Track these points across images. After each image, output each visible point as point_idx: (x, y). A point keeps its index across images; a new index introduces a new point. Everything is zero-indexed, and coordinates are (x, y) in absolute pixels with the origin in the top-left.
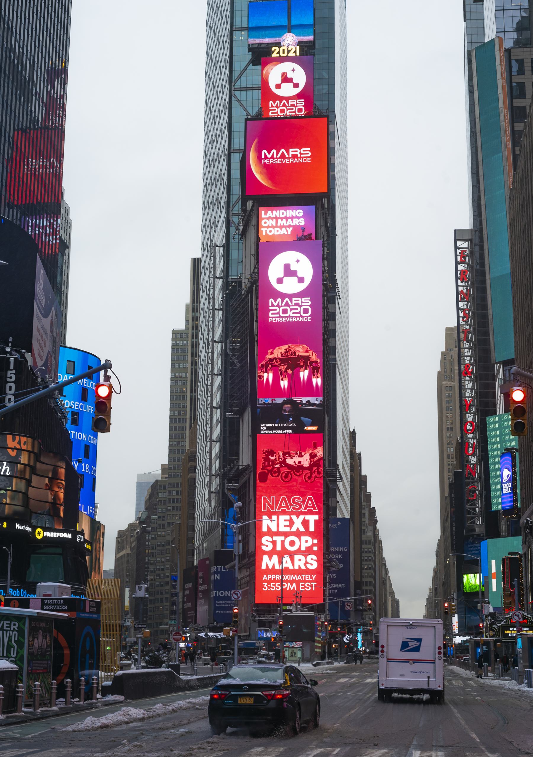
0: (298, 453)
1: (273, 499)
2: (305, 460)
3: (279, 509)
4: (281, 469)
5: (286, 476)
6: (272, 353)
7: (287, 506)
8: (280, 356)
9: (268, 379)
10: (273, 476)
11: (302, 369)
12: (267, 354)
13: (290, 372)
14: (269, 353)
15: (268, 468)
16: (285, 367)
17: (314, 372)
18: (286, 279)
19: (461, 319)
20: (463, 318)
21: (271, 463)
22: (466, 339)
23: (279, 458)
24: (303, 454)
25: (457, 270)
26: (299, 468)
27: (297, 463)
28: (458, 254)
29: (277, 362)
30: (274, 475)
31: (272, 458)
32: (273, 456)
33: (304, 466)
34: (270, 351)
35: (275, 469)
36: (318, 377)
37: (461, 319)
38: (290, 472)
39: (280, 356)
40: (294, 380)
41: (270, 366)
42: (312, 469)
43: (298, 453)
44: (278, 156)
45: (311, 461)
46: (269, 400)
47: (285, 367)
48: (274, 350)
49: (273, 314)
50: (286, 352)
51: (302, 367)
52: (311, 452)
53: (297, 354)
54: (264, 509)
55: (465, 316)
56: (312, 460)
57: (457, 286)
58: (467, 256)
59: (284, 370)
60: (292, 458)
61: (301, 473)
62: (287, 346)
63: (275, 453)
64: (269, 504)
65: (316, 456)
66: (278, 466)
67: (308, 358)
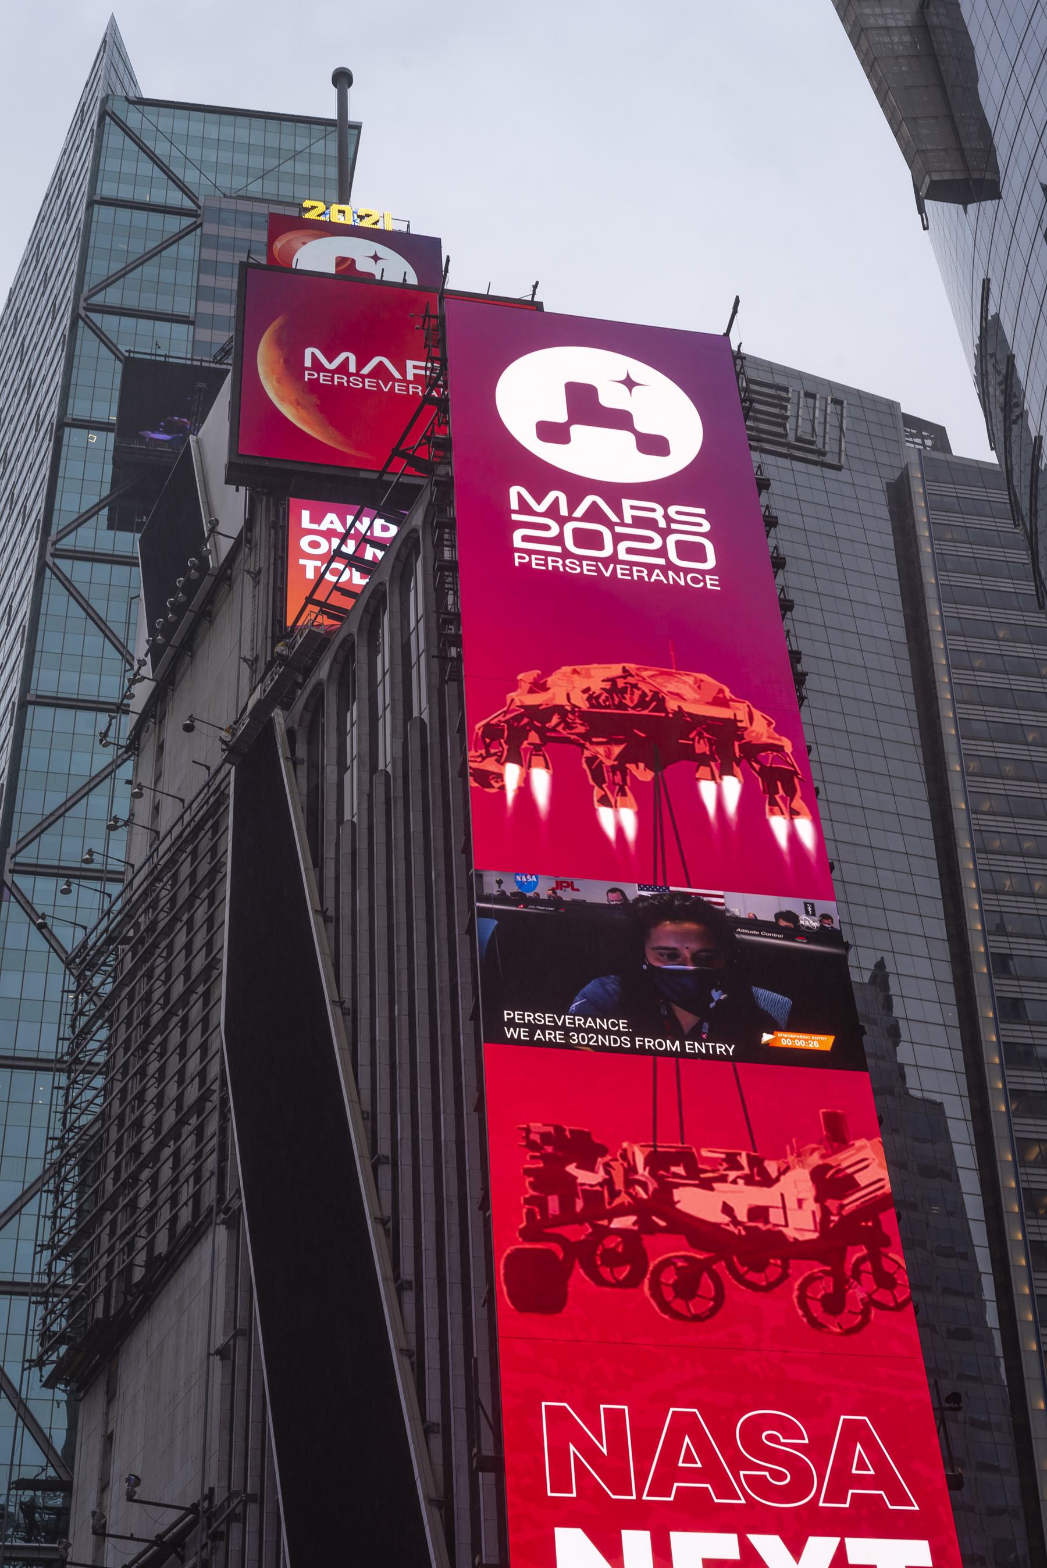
0: (743, 1160)
1: (615, 1418)
2: (791, 1204)
3: (661, 1487)
4: (647, 1241)
5: (687, 1287)
6: (539, 686)
7: (711, 1471)
8: (584, 705)
9: (525, 790)
10: (600, 1281)
11: (703, 770)
12: (514, 686)
13: (643, 774)
14: (526, 686)
15: (565, 1231)
16: (617, 750)
17: (772, 791)
18: (575, 430)
21: (579, 1205)
23: (630, 1182)
24: (772, 1167)
26: (758, 1243)
27: (742, 1216)
29: (569, 726)
30: (605, 1272)
31: (586, 1178)
32: (592, 1169)
33: (790, 1233)
34: (526, 677)
35: (612, 1243)
36: (793, 813)
38: (705, 1266)
39: (584, 705)
40: (669, 810)
41: (534, 737)
42: (842, 1259)
43: (743, 1160)
44: (365, 371)
45: (826, 1212)
46: (543, 886)
47: (617, 750)
48: (548, 672)
49: (526, 539)
50: (613, 688)
51: (703, 760)
52: (815, 1160)
53: (672, 705)
54: (561, 1483)
56: (832, 1204)
59: (608, 763)
60: (707, 1185)
61: (774, 1271)
62: (616, 670)
63: (603, 1151)
64: (589, 1450)
65: (849, 1184)
66: (624, 1222)
67: (730, 729)
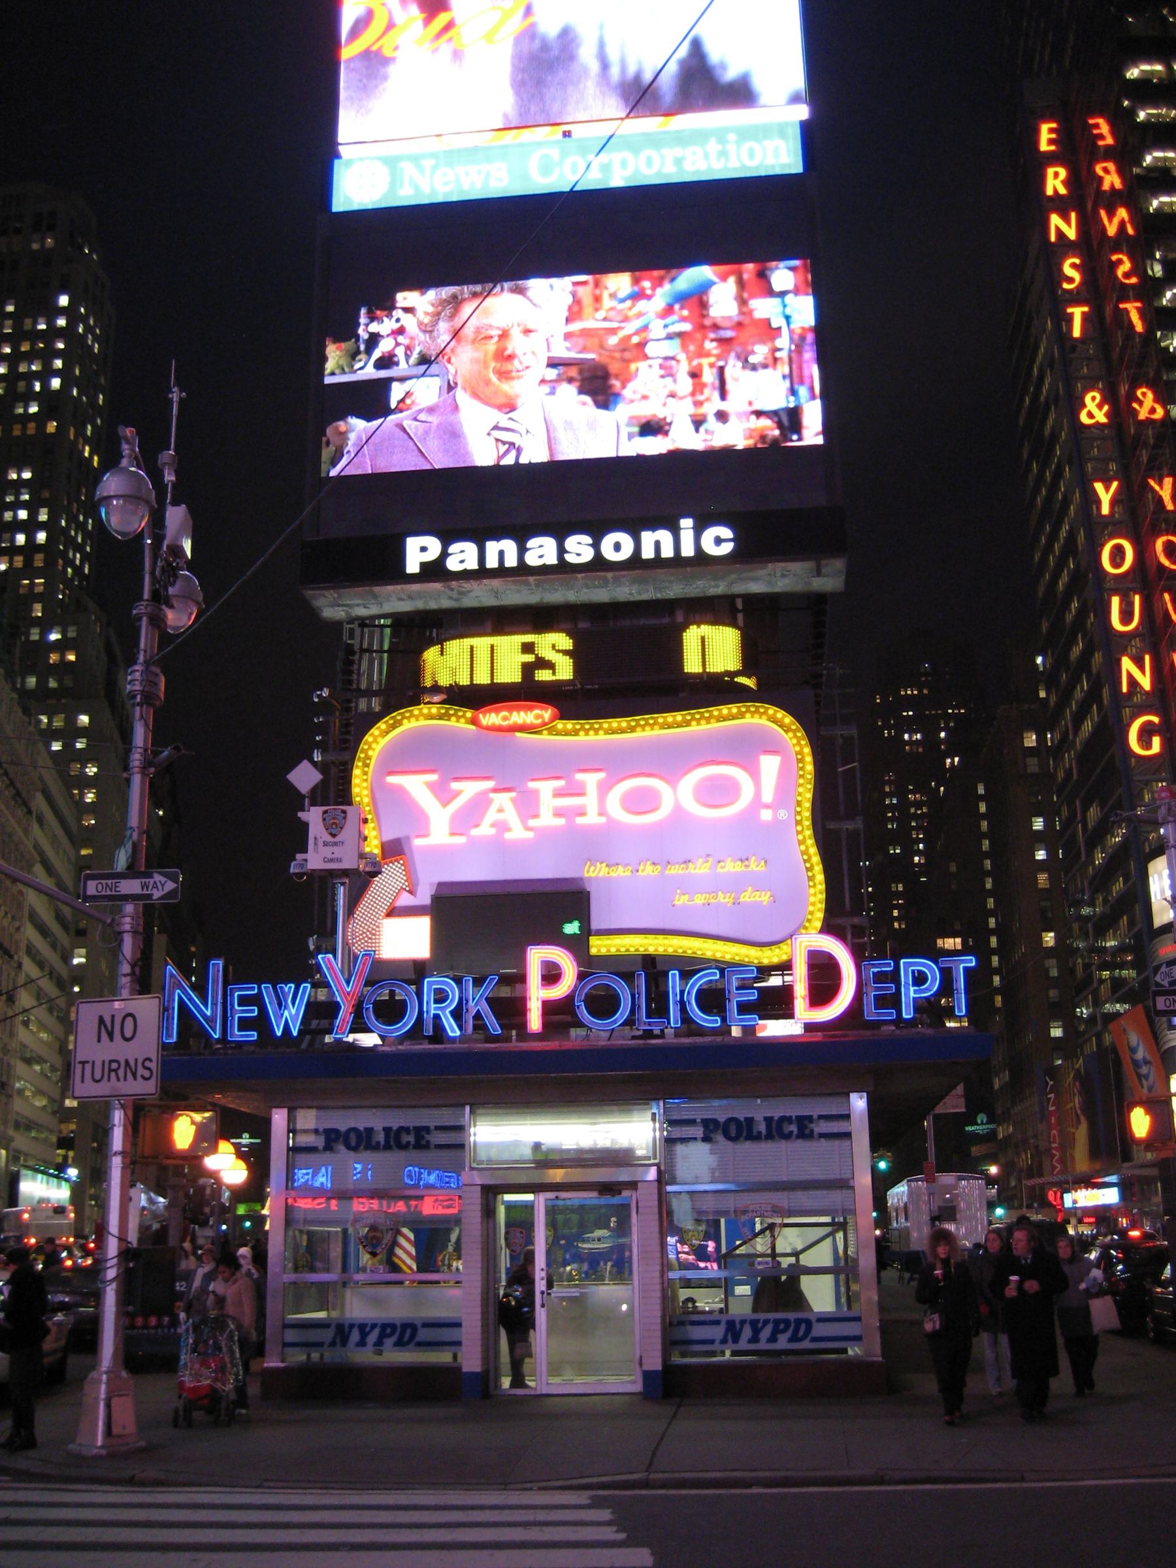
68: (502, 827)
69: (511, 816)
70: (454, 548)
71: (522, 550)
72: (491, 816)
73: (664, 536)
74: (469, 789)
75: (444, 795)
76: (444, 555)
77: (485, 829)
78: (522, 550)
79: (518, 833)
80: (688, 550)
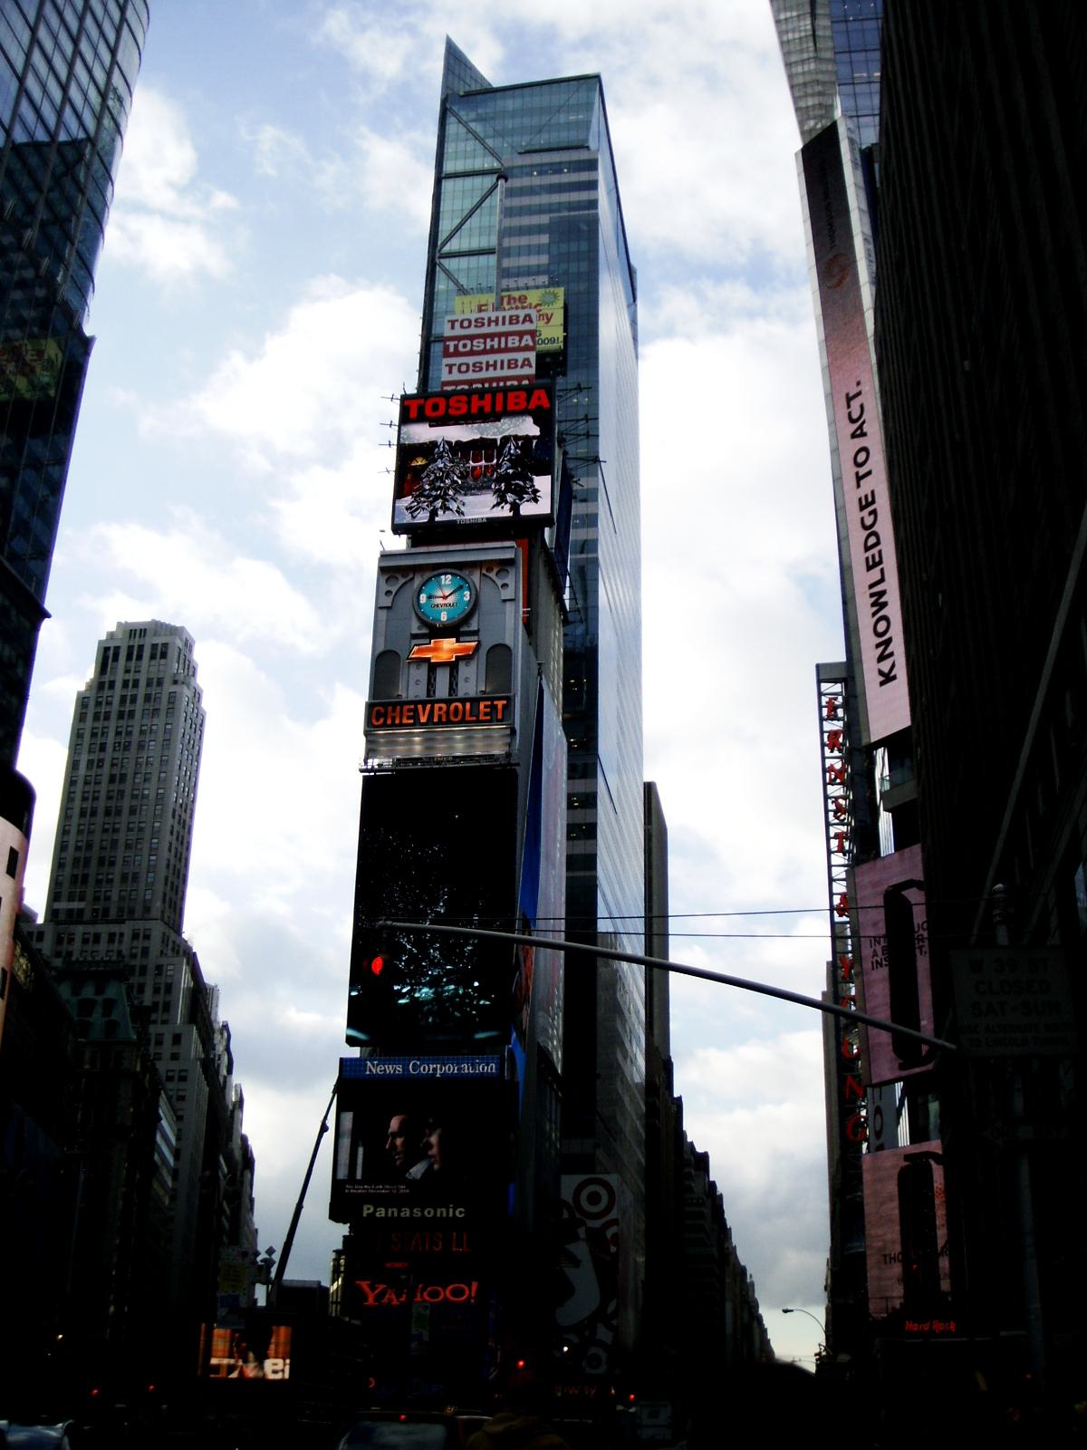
19: (831, 814)
20: (836, 812)
22: (841, 849)
25: (822, 732)
28: (824, 704)
37: (831, 814)
55: (839, 809)
57: (824, 758)
58: (837, 707)
68: (390, 1300)
69: (394, 1297)
70: (378, 1209)
71: (399, 1212)
72: (387, 1296)
73: (444, 1210)
74: (382, 1287)
75: (373, 1288)
76: (375, 1211)
77: (385, 1300)
78: (399, 1212)
79: (395, 1302)
80: (451, 1214)
